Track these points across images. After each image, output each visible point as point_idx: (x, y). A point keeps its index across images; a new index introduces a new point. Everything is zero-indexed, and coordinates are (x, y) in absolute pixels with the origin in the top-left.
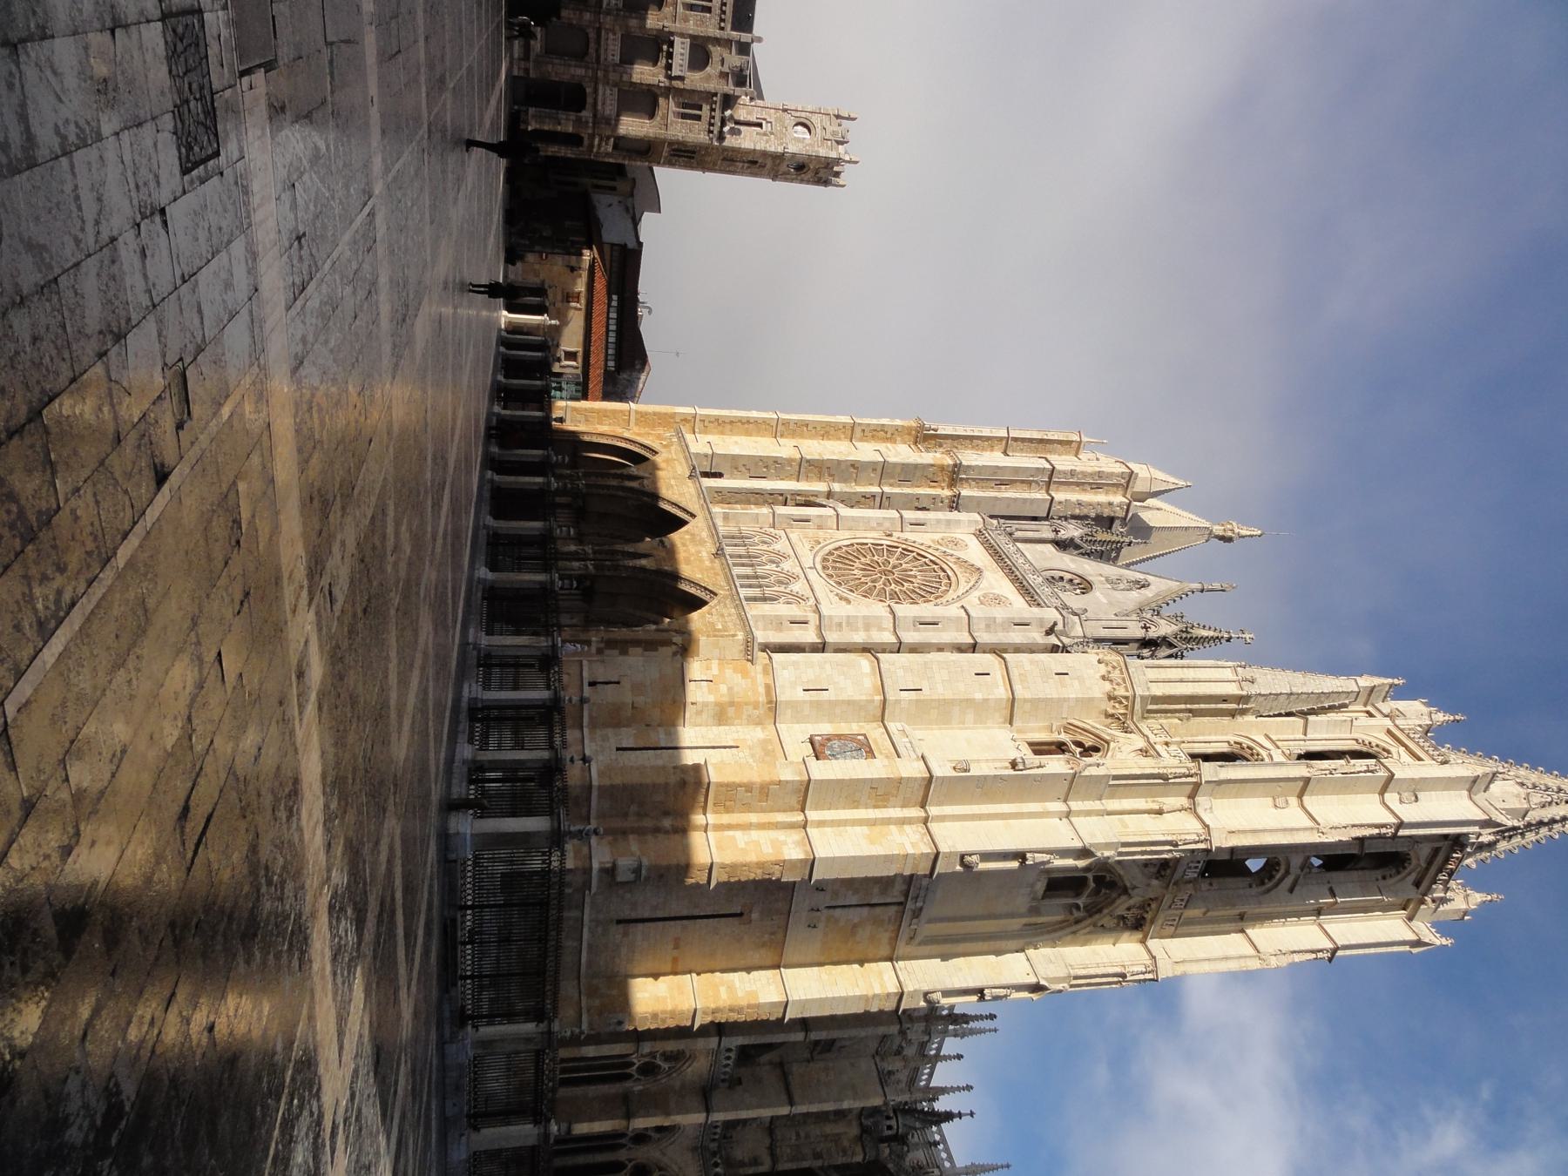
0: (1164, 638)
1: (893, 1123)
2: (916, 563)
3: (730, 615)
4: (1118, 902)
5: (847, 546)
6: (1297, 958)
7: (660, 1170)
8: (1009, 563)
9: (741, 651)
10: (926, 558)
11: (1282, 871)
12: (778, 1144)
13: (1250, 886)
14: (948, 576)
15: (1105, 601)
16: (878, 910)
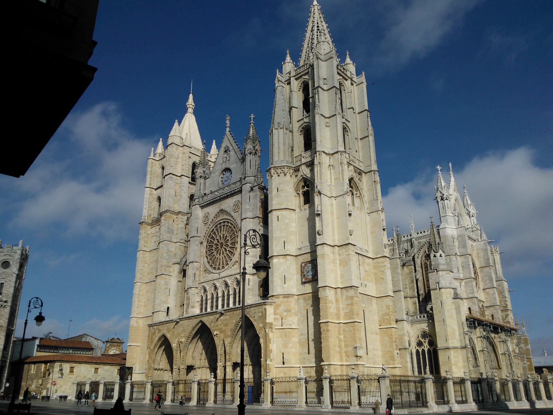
0: (254, 147)
1: (401, 254)
2: (217, 233)
3: (255, 310)
4: (355, 181)
5: (207, 259)
6: (370, 123)
7: (419, 337)
8: (218, 198)
9: (271, 307)
10: (213, 229)
11: (344, 124)
12: (409, 295)
13: (348, 135)
14: (223, 222)
15: (235, 165)
16: (360, 263)
